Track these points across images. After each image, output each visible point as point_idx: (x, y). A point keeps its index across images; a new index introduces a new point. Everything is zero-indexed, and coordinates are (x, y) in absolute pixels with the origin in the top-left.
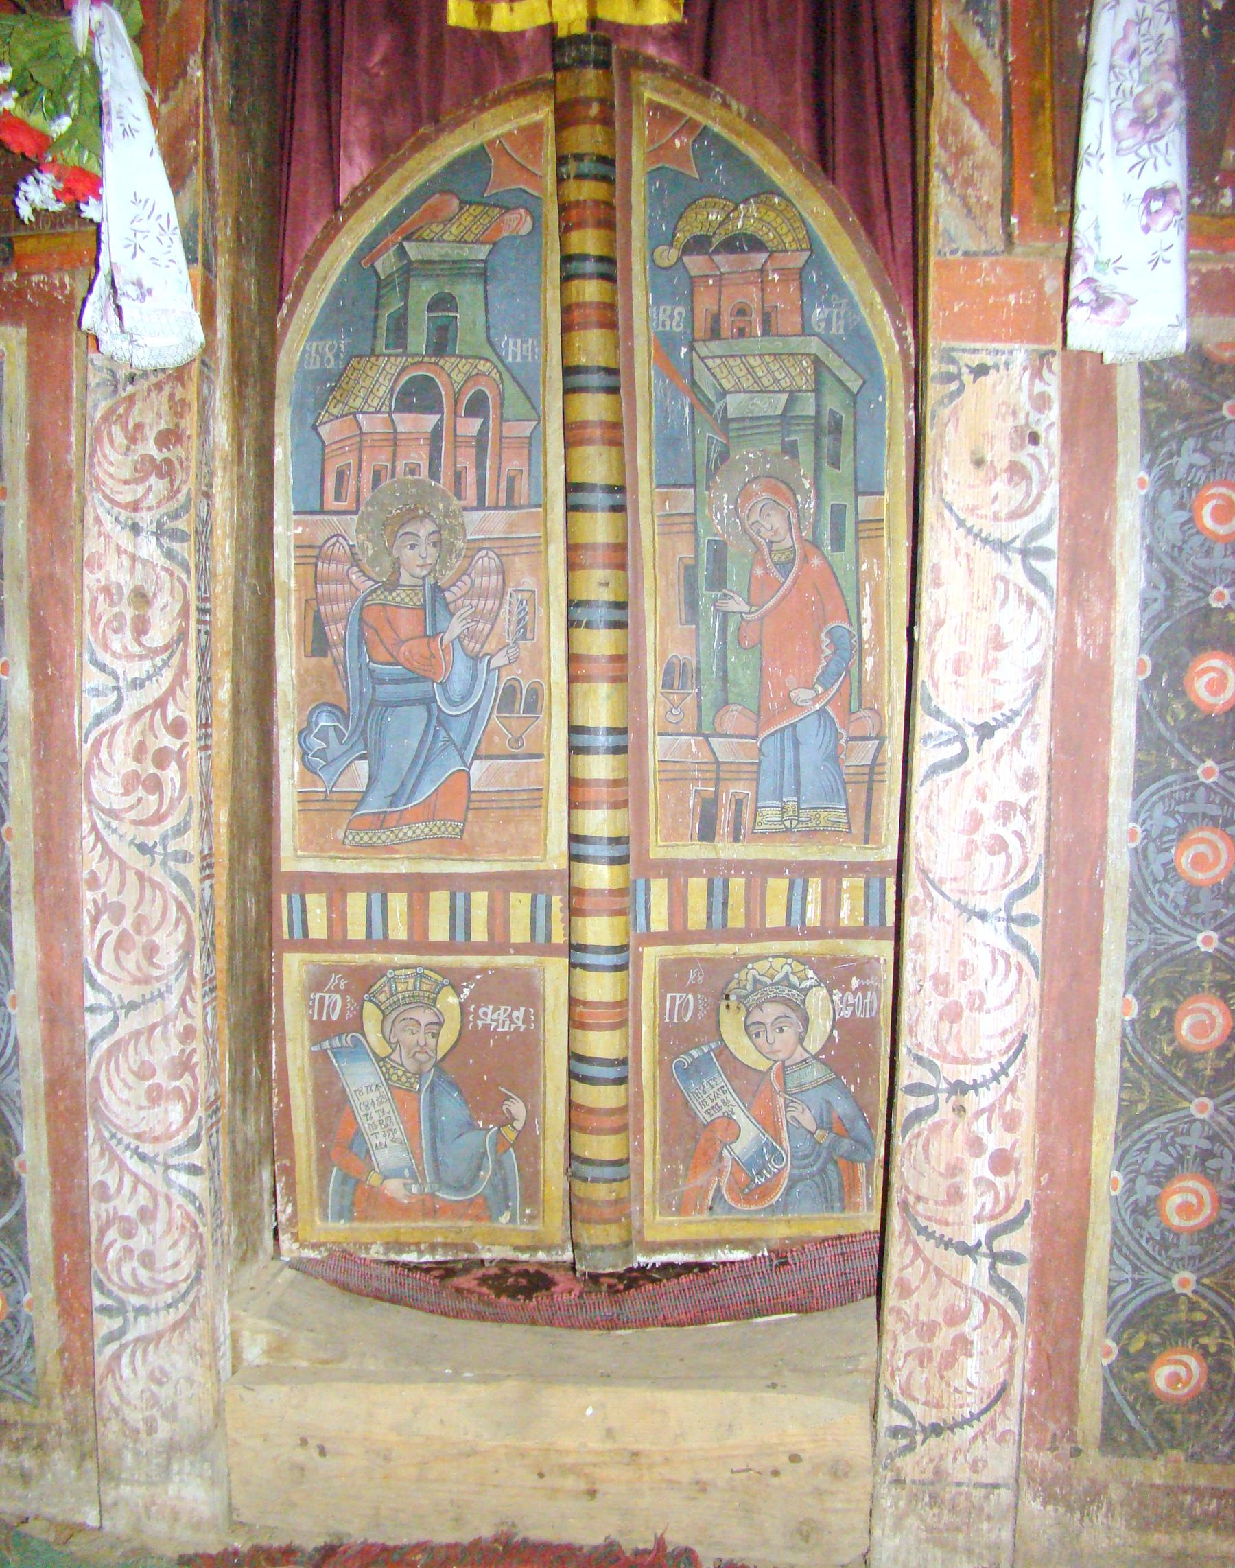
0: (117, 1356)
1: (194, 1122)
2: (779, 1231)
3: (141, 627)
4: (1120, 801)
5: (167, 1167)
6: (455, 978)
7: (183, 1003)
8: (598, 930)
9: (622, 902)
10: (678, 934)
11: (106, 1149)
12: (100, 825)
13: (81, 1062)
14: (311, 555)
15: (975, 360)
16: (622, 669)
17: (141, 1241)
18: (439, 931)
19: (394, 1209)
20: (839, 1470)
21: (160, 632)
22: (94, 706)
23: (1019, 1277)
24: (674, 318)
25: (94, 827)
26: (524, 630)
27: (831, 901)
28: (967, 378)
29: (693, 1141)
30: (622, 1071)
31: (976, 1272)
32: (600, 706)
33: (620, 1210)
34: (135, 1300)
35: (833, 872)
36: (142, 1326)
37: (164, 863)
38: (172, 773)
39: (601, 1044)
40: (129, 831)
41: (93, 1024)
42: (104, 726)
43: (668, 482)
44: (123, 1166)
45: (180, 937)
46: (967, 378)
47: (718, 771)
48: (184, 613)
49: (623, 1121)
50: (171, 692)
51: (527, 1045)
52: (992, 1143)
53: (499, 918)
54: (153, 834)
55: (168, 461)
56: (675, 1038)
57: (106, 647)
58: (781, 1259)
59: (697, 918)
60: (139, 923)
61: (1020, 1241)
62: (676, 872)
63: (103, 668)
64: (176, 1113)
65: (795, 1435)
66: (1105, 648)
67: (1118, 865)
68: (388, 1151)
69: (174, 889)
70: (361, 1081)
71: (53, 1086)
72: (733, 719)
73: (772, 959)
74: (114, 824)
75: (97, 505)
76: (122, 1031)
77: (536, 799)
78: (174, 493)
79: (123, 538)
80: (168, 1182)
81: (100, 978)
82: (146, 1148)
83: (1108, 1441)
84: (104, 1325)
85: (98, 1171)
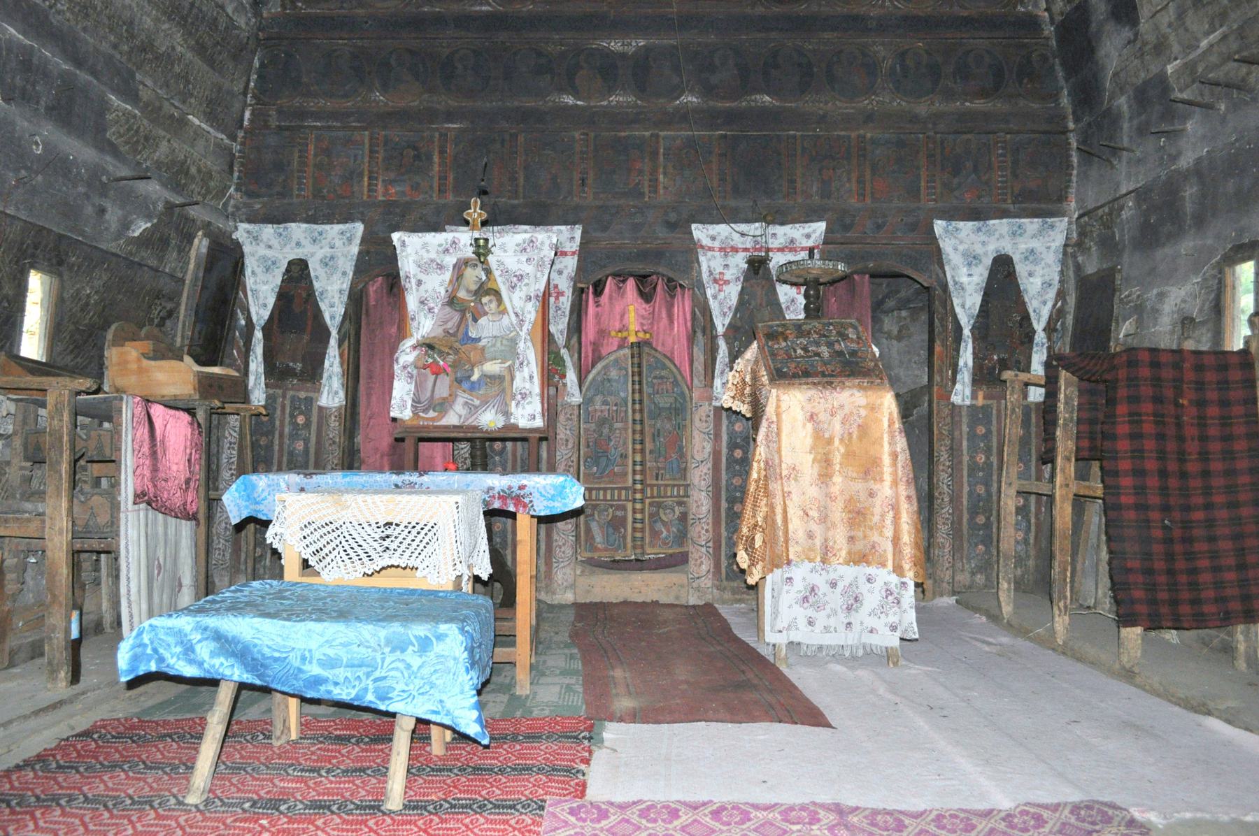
2: (670, 551)
4: (724, 472)
6: (611, 506)
8: (638, 496)
9: (642, 491)
14: (586, 430)
16: (642, 451)
19: (599, 550)
20: (682, 586)
21: (570, 446)
23: (711, 550)
24: (650, 390)
26: (625, 443)
29: (655, 534)
30: (642, 521)
31: (704, 550)
33: (642, 547)
35: (679, 486)
39: (639, 516)
47: (659, 468)
51: (624, 518)
53: (620, 495)
56: (651, 515)
58: (671, 555)
61: (710, 544)
62: (652, 486)
65: (675, 580)
67: (724, 483)
68: (599, 539)
72: (661, 459)
73: (669, 501)
77: (626, 474)
83: (727, 579)
85: (555, 537)
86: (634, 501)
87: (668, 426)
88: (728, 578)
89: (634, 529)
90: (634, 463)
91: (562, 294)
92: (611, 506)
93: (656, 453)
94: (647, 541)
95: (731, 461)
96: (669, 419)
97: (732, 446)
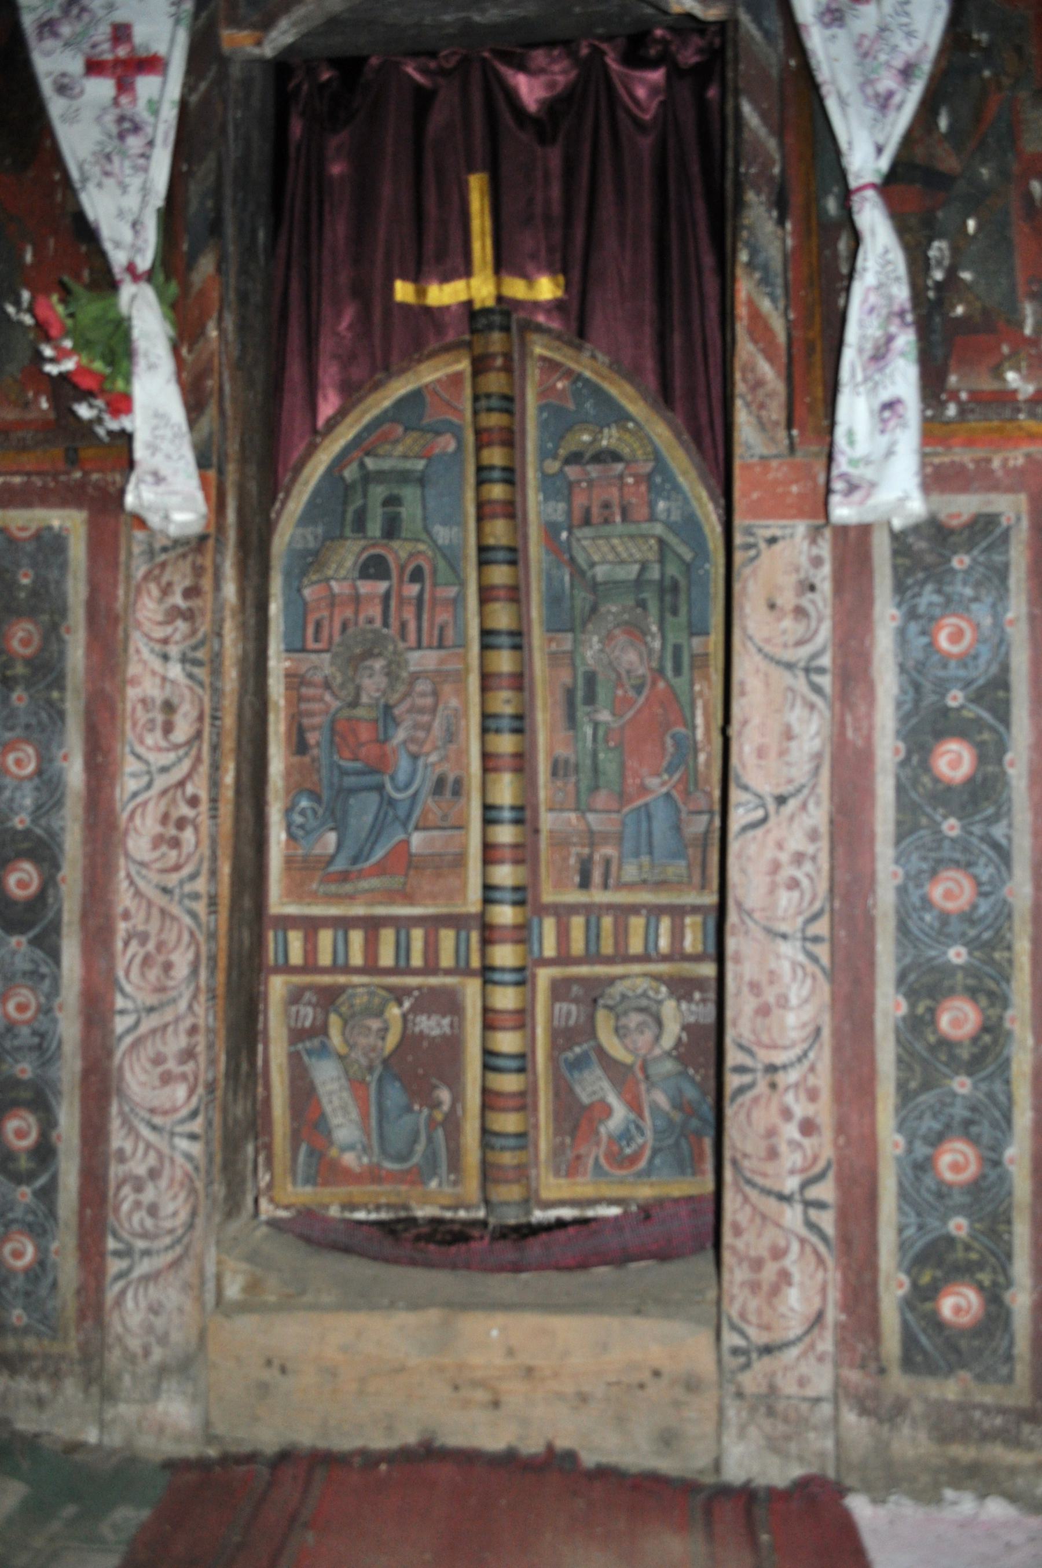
0: (123, 1293)
1: (195, 1100)
2: (645, 1192)
3: (168, 728)
4: (885, 850)
5: (172, 1134)
6: (398, 995)
7: (190, 1007)
8: (504, 955)
9: (522, 934)
10: (563, 958)
11: (126, 1122)
12: (133, 872)
13: (110, 1054)
14: (295, 681)
15: (768, 533)
16: (522, 763)
17: (149, 1195)
18: (386, 958)
19: (347, 1176)
20: (692, 1385)
21: (182, 731)
22: (132, 785)
23: (827, 1221)
24: (557, 511)
25: (128, 876)
26: (451, 735)
27: (677, 934)
28: (762, 545)
29: (576, 1118)
30: (523, 1062)
31: (792, 1216)
32: (505, 791)
33: (522, 1173)
34: (140, 1244)
35: (677, 912)
36: (144, 1267)
37: (180, 902)
38: (188, 835)
39: (507, 1042)
40: (155, 877)
41: (121, 1024)
42: (140, 799)
43: (553, 627)
44: (138, 1136)
45: (190, 955)
46: (762, 545)
47: (592, 839)
48: (200, 718)
49: (524, 1102)
50: (189, 776)
52: (800, 1109)
53: (431, 949)
54: (172, 880)
55: (190, 610)
56: (562, 1038)
57: (142, 742)
58: (647, 1212)
59: (577, 946)
60: (160, 946)
61: (825, 1191)
62: (562, 913)
63: (138, 757)
64: (181, 1091)
65: (656, 1354)
66: (869, 739)
67: (885, 899)
69: (187, 920)
70: (327, 1075)
71: (87, 1073)
72: (602, 799)
73: (634, 980)
74: (144, 872)
75: (137, 640)
76: (143, 1028)
77: (459, 861)
78: (194, 632)
79: (156, 664)
80: (173, 1147)
81: (128, 988)
82: (158, 1120)
83: (908, 1363)
84: (115, 1266)
85: (118, 1139)
86: (487, 973)
87: (630, 658)
88: (913, 1359)
89: (490, 1099)
90: (490, 815)
91: (152, 64)
92: (398, 995)
93: (582, 778)
94: (544, 1145)
95: (921, 795)
96: (637, 631)
97: (927, 725)
